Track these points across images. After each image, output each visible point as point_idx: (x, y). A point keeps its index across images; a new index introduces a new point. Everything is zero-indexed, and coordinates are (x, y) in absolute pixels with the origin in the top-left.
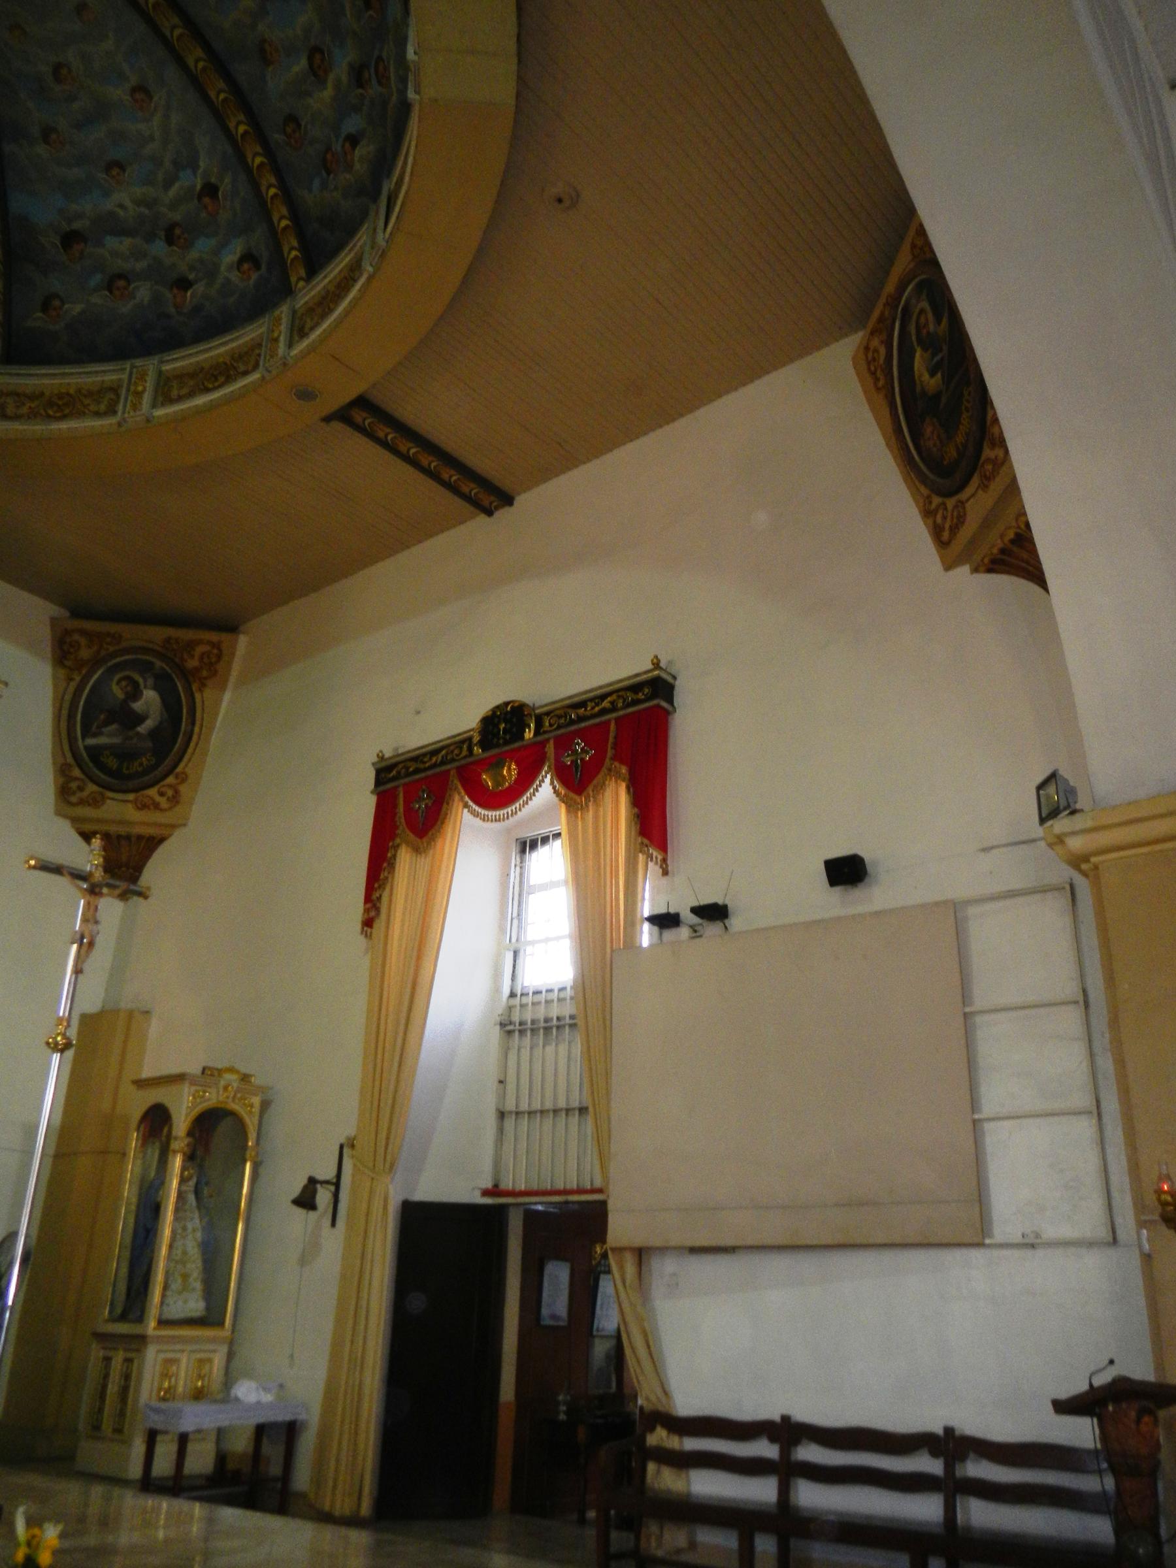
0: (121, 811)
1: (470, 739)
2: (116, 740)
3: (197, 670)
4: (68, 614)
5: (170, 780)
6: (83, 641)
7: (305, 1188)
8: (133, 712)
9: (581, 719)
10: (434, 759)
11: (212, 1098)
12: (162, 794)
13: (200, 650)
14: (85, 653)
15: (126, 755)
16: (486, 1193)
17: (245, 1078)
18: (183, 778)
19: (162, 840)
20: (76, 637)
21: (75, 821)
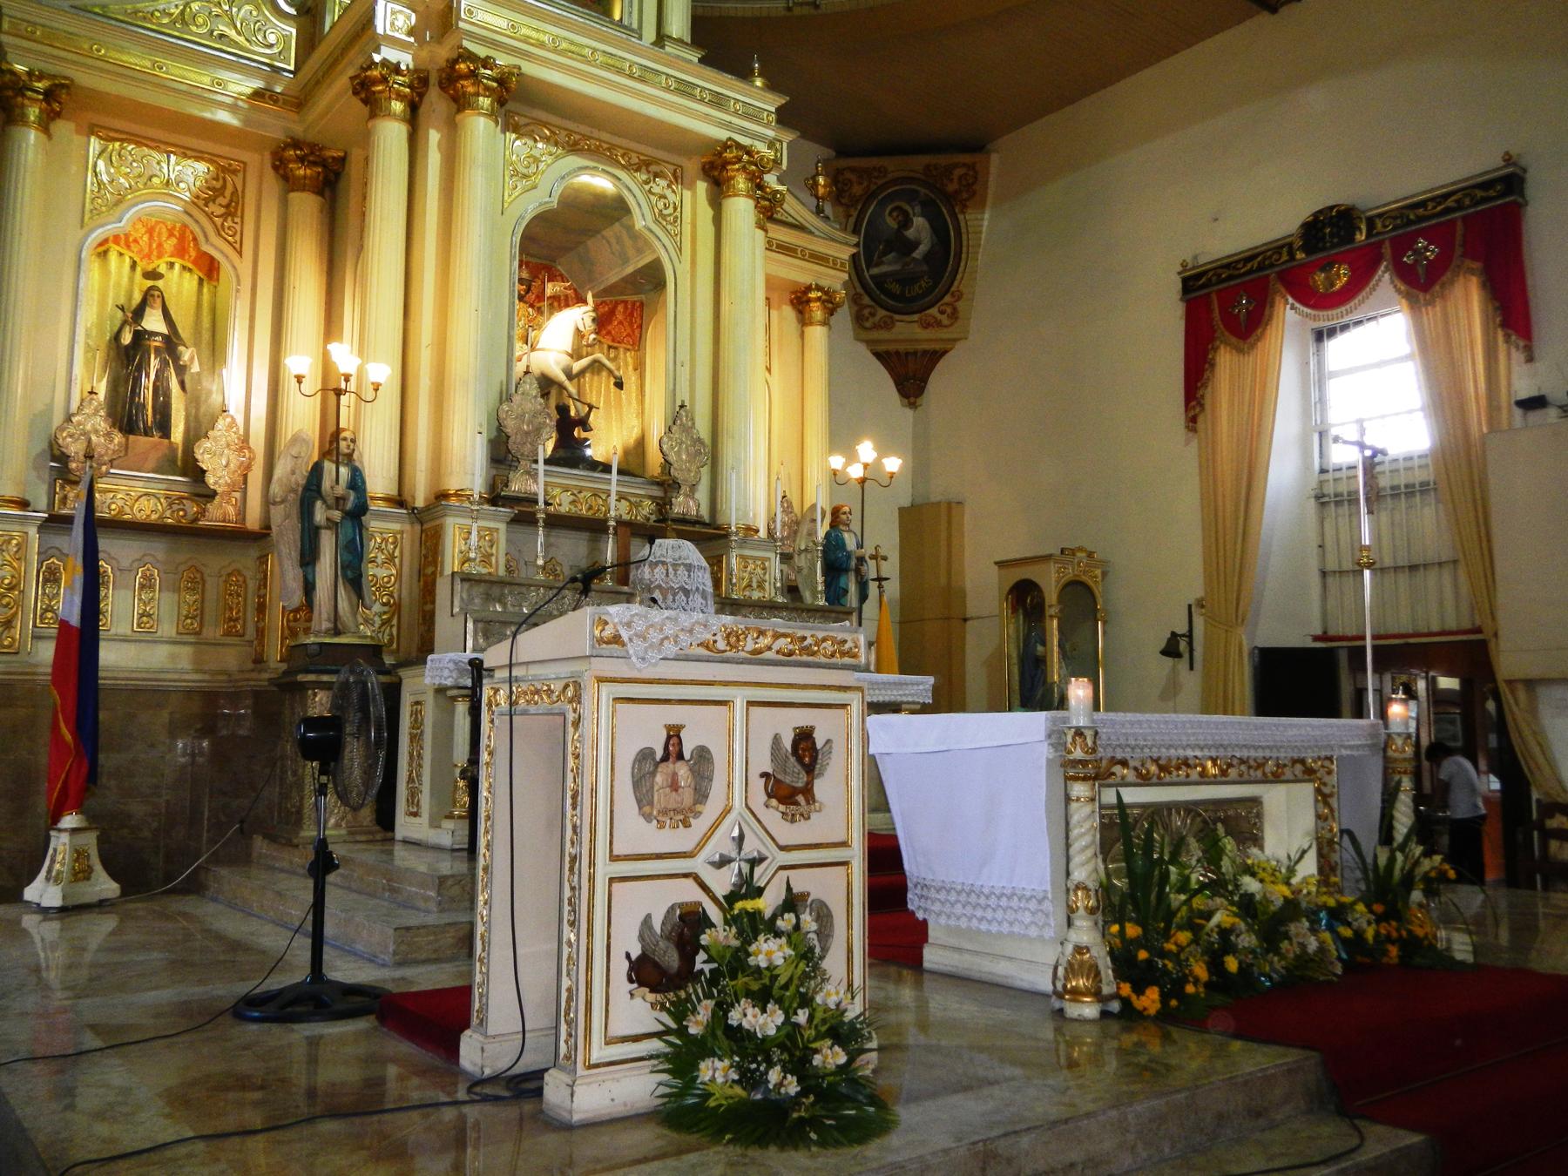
0: (908, 332)
1: (1290, 245)
2: (896, 267)
3: (956, 192)
4: (830, 153)
5: (947, 299)
6: (853, 177)
7: (1169, 640)
8: (908, 240)
9: (1420, 219)
10: (1249, 266)
11: (1070, 573)
12: (942, 312)
13: (958, 172)
14: (857, 190)
15: (906, 280)
16: (1316, 638)
17: (1090, 555)
18: (959, 296)
19: (945, 352)
20: (848, 175)
21: (868, 342)
